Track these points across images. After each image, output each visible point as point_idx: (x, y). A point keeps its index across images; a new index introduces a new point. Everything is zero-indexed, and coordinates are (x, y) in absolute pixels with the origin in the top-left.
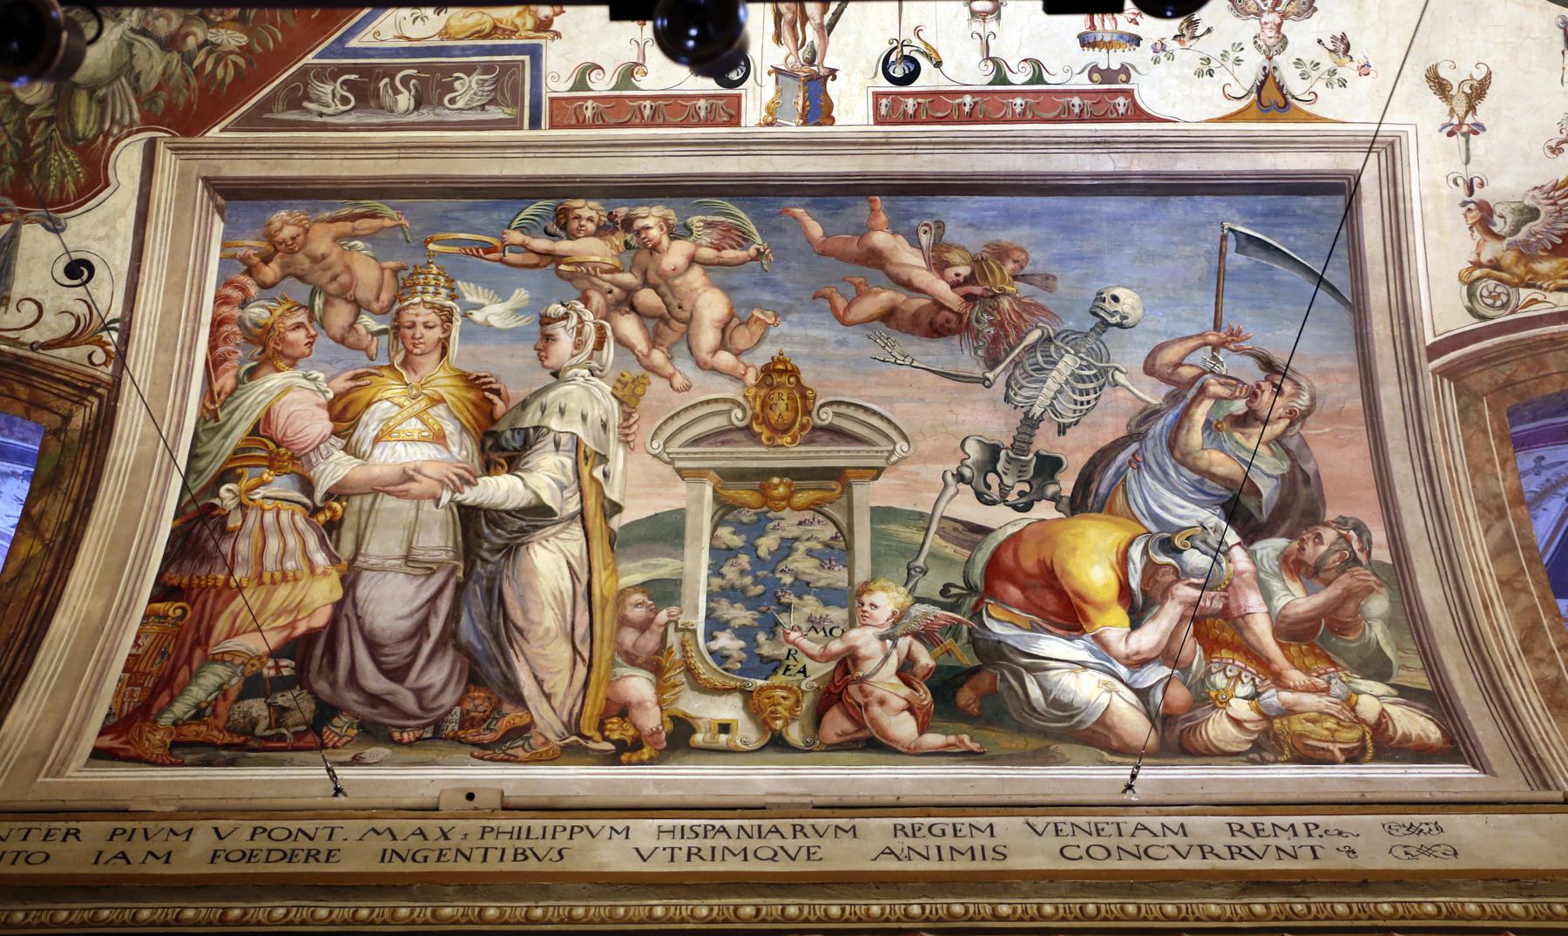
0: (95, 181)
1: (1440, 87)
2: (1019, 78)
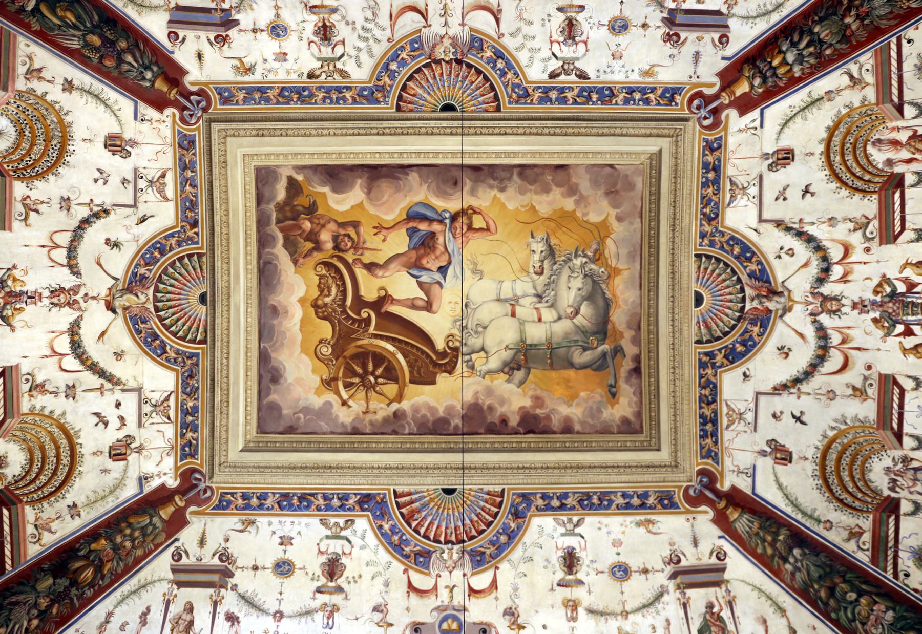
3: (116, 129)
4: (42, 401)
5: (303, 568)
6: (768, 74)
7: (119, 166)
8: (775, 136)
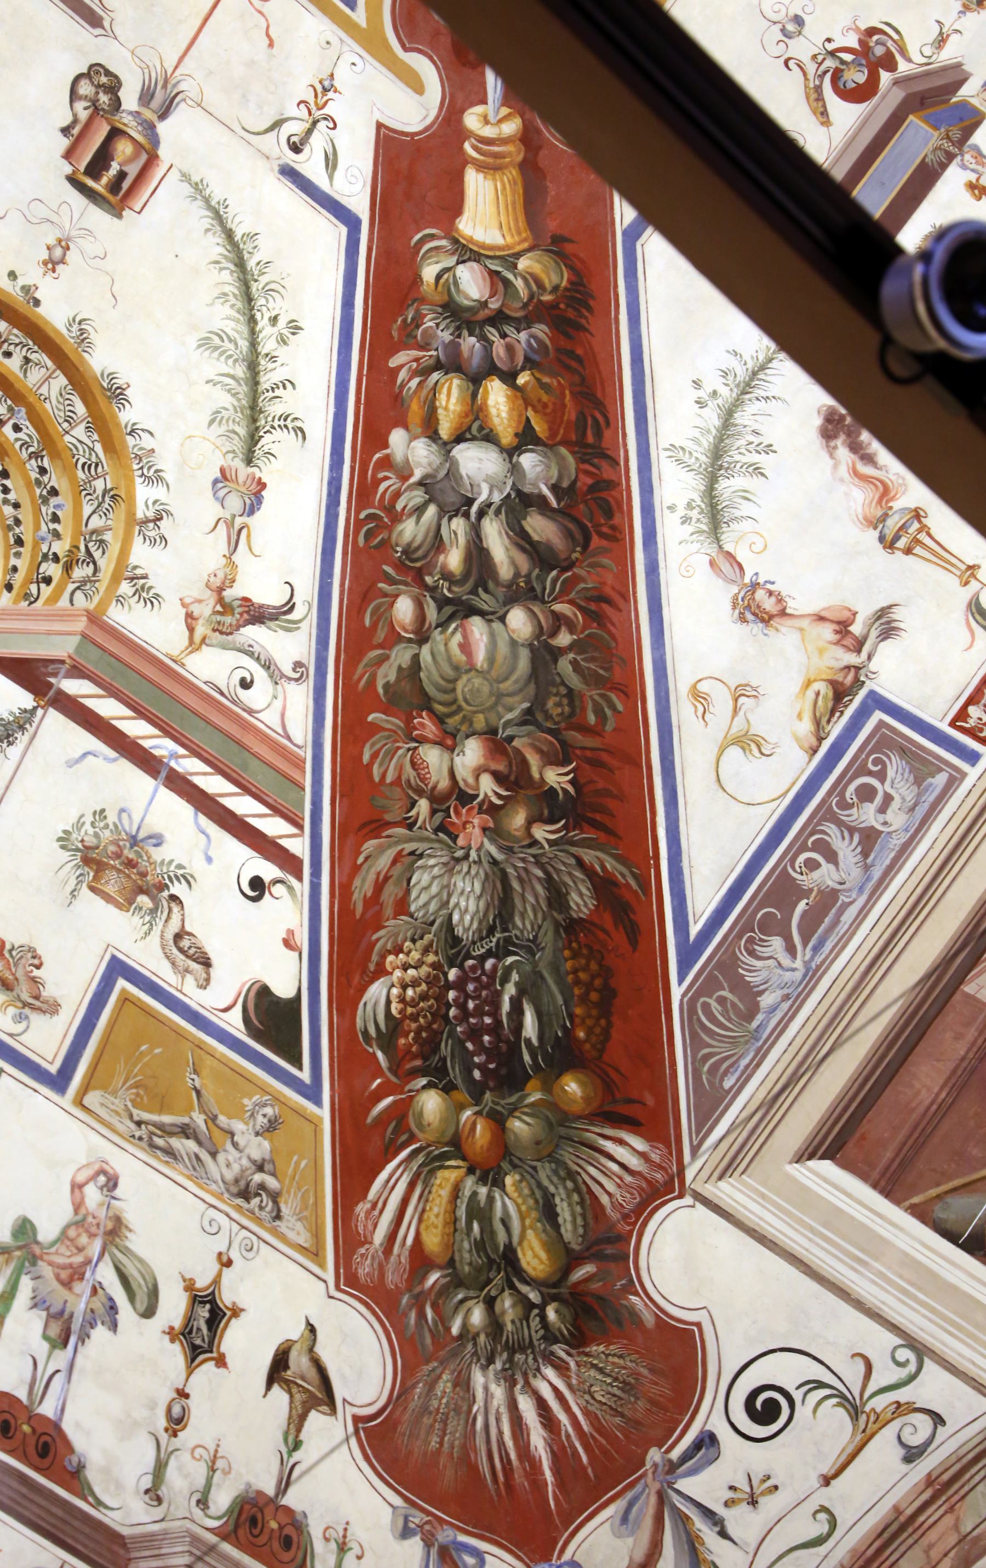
6: (470, 343)
8: (217, 193)
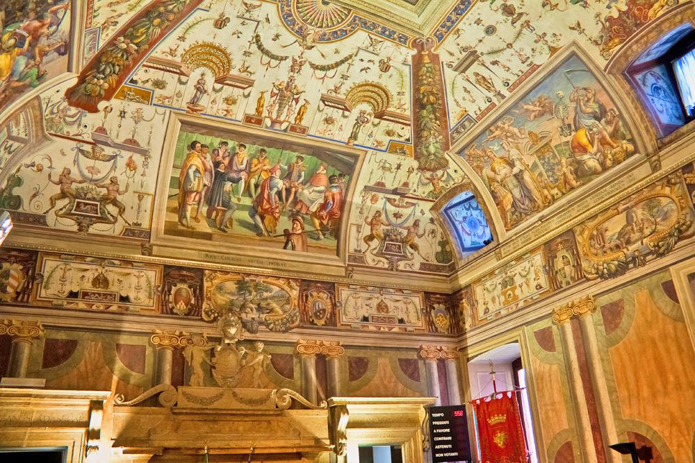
0: (447, 161)
1: (573, 28)
2: (520, 74)
3: (212, 22)
4: (343, 90)
5: (498, 22)
7: (234, 24)
